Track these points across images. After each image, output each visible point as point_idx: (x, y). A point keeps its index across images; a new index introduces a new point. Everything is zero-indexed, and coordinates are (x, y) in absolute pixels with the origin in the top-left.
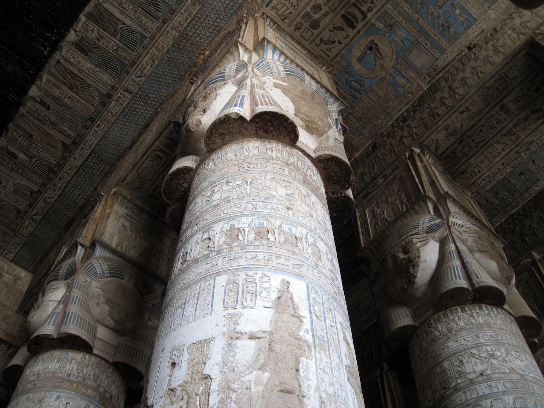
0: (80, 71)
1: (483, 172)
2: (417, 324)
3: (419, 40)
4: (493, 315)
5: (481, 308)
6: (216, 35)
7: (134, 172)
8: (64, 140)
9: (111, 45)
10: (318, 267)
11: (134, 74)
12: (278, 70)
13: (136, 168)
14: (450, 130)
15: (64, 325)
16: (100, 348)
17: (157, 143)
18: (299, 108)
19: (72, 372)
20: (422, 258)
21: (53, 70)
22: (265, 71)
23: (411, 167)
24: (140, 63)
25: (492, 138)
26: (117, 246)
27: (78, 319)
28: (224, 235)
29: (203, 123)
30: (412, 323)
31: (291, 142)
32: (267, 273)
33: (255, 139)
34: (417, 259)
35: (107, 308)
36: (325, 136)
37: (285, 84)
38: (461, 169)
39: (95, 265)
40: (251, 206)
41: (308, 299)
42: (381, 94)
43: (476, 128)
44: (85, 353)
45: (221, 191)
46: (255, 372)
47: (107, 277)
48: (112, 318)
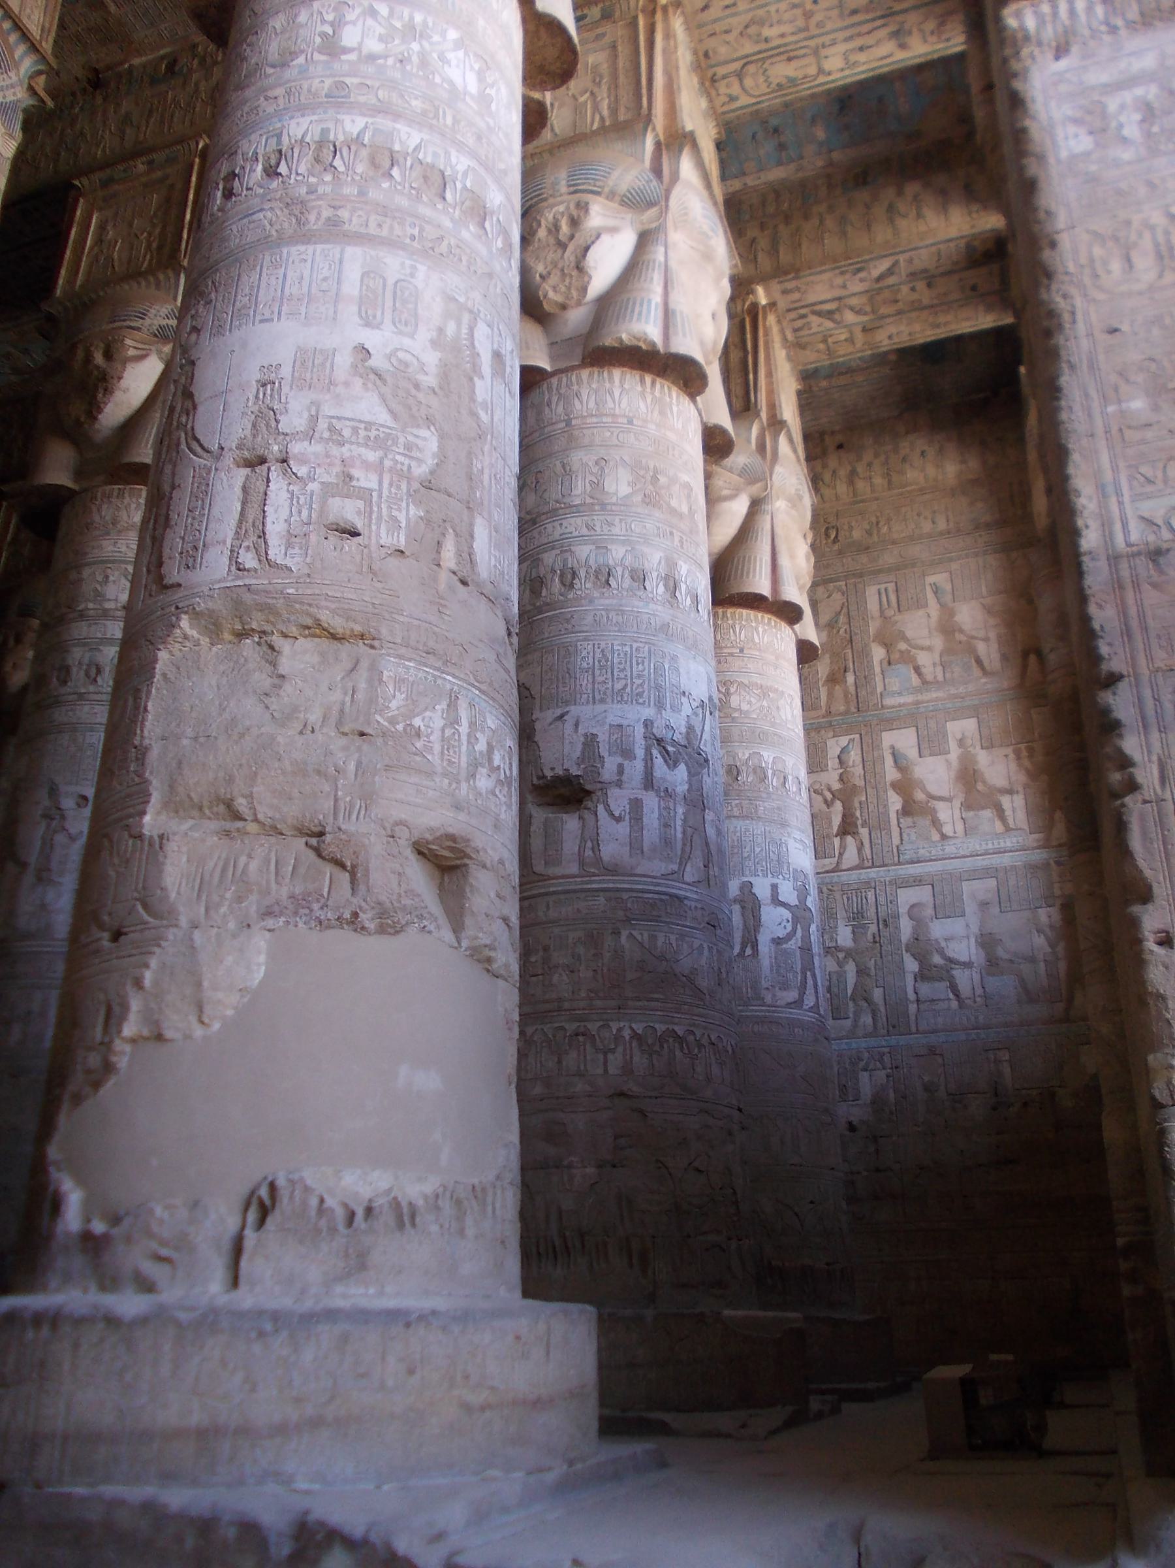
20: (123, 383)
23: (194, 179)
34: (115, 381)
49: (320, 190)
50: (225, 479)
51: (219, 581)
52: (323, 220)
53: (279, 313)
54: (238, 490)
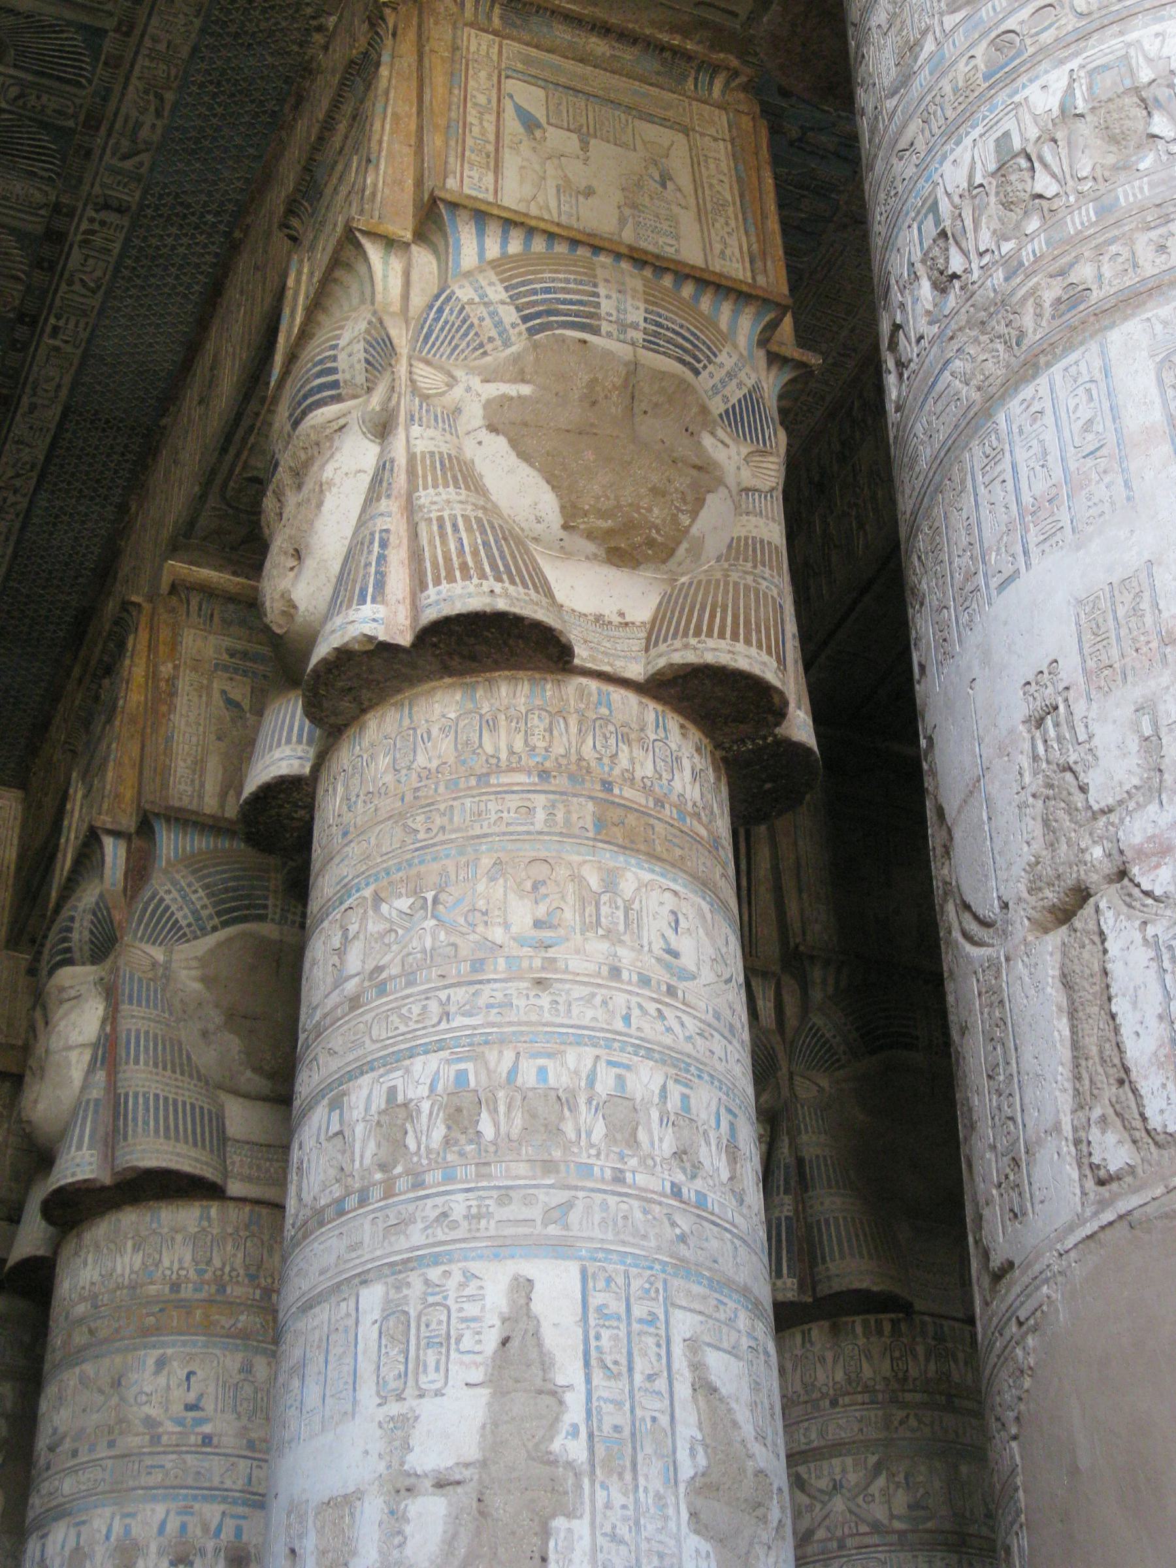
7: (213, 501)
11: (108, 152)
12: (498, 324)
15: (122, 1143)
16: (246, 1171)
18: (573, 497)
19: (183, 1273)
22: (457, 346)
24: (116, 114)
27: (157, 1109)
29: (302, 608)
31: (557, 662)
33: (448, 680)
35: (233, 1044)
36: (685, 545)
37: (526, 390)
41: (585, 1318)
44: (205, 1203)
45: (362, 936)
47: (215, 929)
48: (257, 1070)
49: (1027, 256)
50: (1025, 972)
51: (1071, 1228)
52: (1048, 311)
53: (1026, 553)
54: (1054, 993)
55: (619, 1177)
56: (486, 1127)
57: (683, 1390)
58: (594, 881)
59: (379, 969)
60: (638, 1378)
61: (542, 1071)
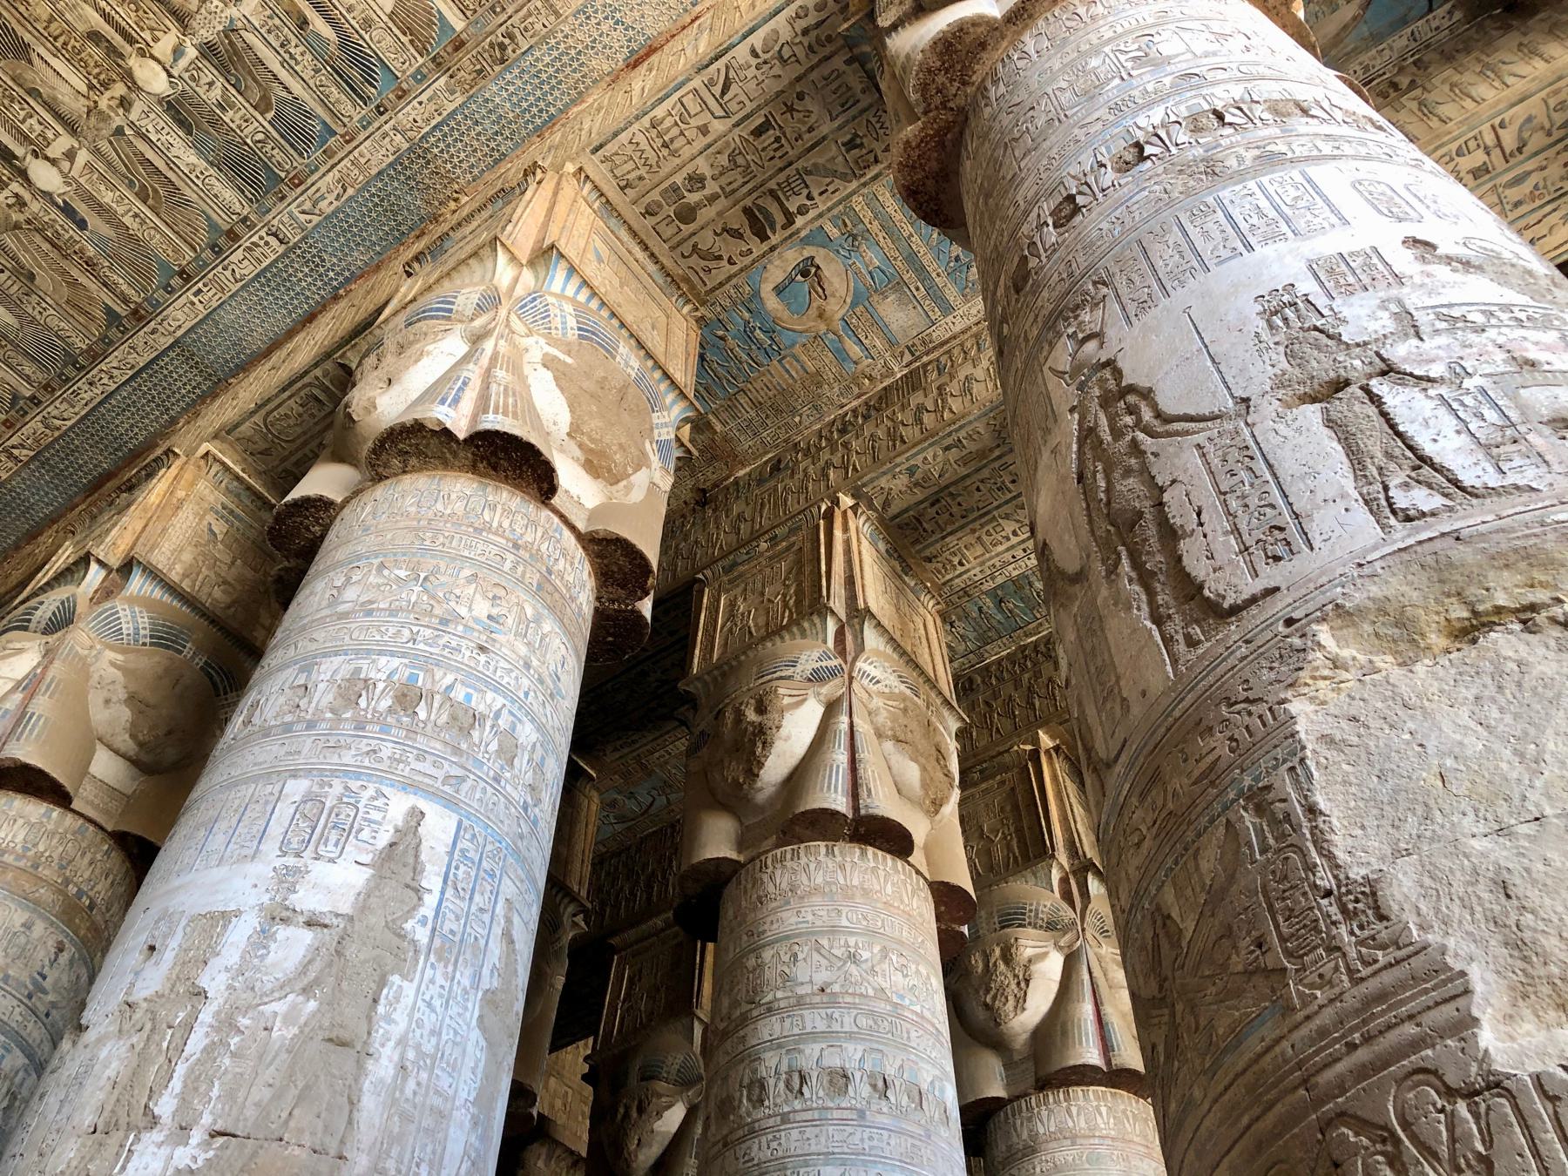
0: (170, 164)
1: (968, 566)
2: (742, 859)
3: (905, 278)
4: (881, 873)
5: (863, 853)
6: (490, 168)
7: (258, 418)
8: (110, 303)
9: (251, 128)
10: (499, 782)
12: (564, 323)
13: (263, 412)
14: (918, 475)
17: (318, 372)
20: (783, 732)
21: (104, 146)
25: (998, 507)
26: (185, 576)
28: (335, 689)
30: (733, 855)
32: (386, 790)
35: (126, 714)
36: (624, 483)
37: (569, 360)
38: (927, 553)
39: (121, 614)
40: (406, 633)
41: (451, 854)
42: (811, 369)
43: (968, 482)
46: (291, 997)
48: (131, 736)
55: (497, 779)
56: (422, 713)
57: (497, 930)
58: (529, 611)
59: (371, 602)
60: (474, 909)
61: (468, 697)
